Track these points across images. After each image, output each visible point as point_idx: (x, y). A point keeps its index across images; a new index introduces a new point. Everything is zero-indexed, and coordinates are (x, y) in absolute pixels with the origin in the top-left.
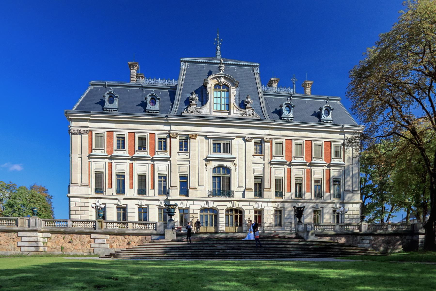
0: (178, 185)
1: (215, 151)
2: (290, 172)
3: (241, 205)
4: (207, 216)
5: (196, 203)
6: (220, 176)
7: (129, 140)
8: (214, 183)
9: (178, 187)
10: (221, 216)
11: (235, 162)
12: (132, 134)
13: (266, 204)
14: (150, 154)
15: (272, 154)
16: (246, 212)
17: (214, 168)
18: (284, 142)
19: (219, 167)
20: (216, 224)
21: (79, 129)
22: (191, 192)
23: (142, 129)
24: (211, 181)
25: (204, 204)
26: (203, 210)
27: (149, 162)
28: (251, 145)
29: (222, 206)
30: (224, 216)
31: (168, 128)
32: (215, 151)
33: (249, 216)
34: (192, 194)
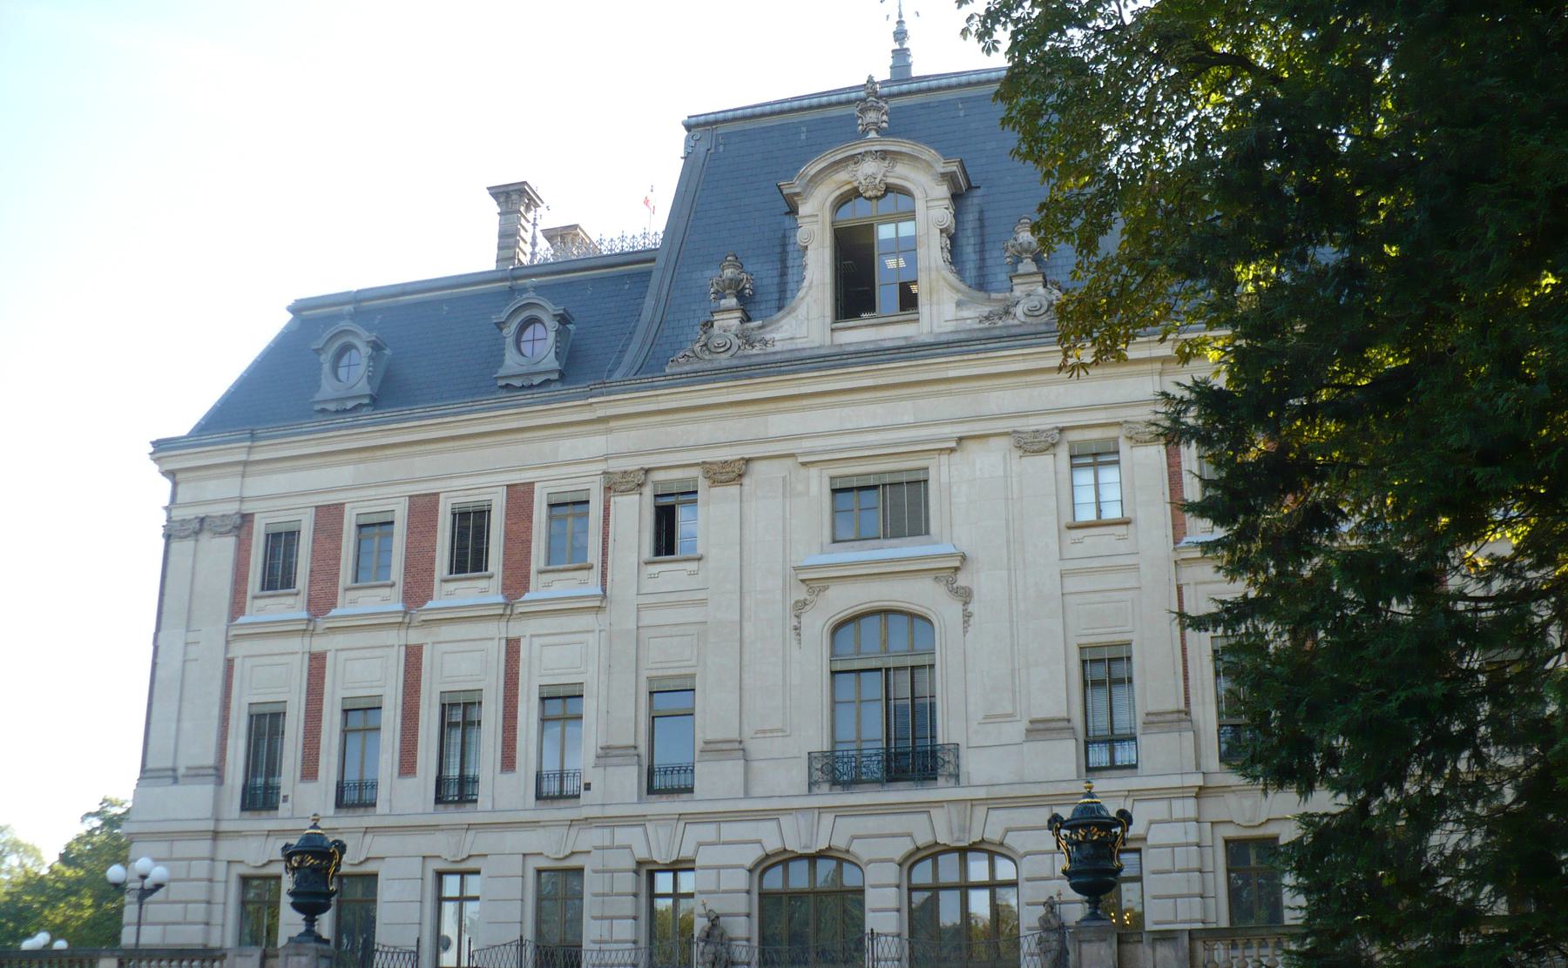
5: (730, 831)
10: (872, 898)
11: (962, 580)
21: (201, 511)
34: (715, 782)
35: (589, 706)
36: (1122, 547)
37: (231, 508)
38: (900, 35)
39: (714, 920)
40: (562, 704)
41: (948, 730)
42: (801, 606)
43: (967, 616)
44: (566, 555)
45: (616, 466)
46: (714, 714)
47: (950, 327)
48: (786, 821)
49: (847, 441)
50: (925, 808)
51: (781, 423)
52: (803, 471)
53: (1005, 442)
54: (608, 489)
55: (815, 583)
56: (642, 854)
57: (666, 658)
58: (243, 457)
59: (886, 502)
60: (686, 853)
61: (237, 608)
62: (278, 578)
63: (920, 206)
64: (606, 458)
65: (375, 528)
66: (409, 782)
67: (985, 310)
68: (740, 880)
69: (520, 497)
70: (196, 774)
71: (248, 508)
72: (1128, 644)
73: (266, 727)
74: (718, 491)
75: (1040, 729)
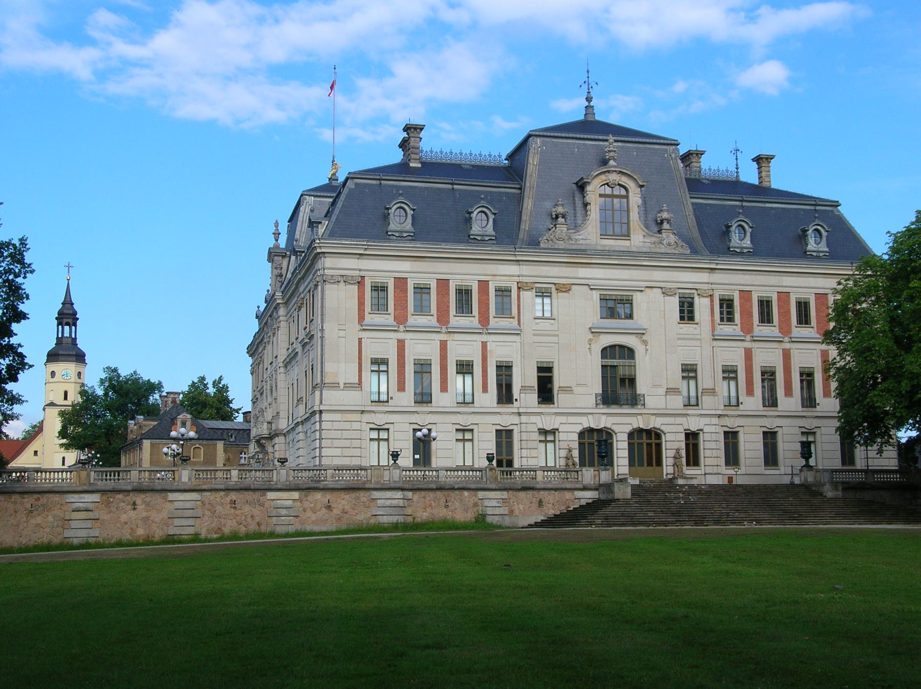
0: (534, 383)
5: (572, 419)
7: (438, 294)
8: (604, 378)
9: (536, 388)
11: (644, 338)
14: (480, 322)
17: (604, 350)
19: (613, 347)
22: (560, 398)
23: (465, 272)
26: (586, 434)
30: (625, 445)
31: (513, 269)
33: (672, 443)
35: (514, 369)
36: (696, 332)
37: (357, 273)
40: (505, 370)
41: (641, 388)
44: (504, 311)
45: (525, 280)
48: (590, 417)
49: (616, 283)
51: (583, 272)
52: (590, 292)
53: (659, 290)
54: (519, 288)
56: (541, 426)
57: (545, 356)
58: (362, 252)
59: (616, 306)
60: (556, 427)
61: (361, 318)
62: (380, 307)
63: (630, 194)
66: (445, 394)
68: (575, 437)
69: (484, 285)
70: (348, 386)
71: (362, 274)
74: (560, 294)
75: (671, 391)
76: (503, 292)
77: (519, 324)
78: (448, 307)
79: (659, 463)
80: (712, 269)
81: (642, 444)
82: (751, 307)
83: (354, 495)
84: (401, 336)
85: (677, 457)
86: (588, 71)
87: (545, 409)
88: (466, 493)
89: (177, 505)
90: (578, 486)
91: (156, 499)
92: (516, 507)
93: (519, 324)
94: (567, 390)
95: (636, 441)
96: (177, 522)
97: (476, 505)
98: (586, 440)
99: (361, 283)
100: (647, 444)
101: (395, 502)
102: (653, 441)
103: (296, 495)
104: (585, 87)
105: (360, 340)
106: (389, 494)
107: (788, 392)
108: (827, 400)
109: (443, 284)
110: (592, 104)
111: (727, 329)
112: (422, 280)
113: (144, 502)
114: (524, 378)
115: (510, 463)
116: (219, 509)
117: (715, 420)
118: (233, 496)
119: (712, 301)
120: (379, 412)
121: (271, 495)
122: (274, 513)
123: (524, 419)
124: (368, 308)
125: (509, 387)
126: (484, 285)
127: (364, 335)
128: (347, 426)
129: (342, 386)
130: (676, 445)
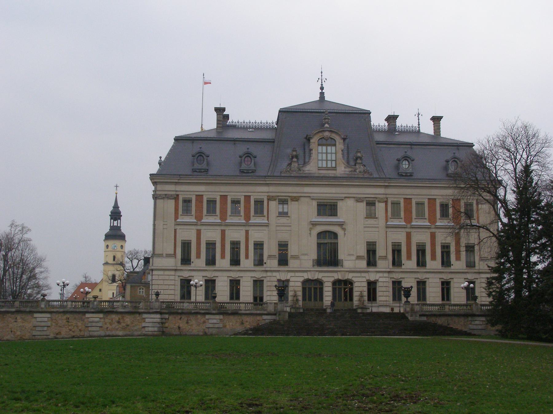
1: (319, 214)
2: (409, 236)
3: (350, 276)
4: (310, 289)
6: (326, 242)
10: (325, 289)
11: (344, 227)
12: (224, 198)
13: (379, 275)
15: (387, 216)
16: (356, 285)
18: (402, 201)
20: (321, 299)
24: (315, 247)
25: (306, 276)
26: (306, 282)
27: (244, 228)
28: (362, 206)
29: (328, 277)
30: (330, 289)
31: (265, 189)
32: (319, 214)
33: (360, 288)
34: (293, 264)
35: (265, 246)
36: (375, 223)
38: (322, 88)
39: (295, 292)
40: (259, 246)
41: (341, 256)
42: (311, 229)
43: (345, 234)
46: (292, 250)
47: (343, 172)
48: (309, 273)
50: (337, 272)
51: (307, 189)
53: (353, 199)
55: (314, 224)
56: (279, 278)
57: (283, 237)
58: (177, 181)
59: (328, 208)
61: (176, 217)
63: (337, 143)
64: (268, 192)
65: (212, 203)
67: (350, 169)
69: (247, 198)
70: (168, 256)
71: (178, 193)
72: (376, 242)
73: (186, 246)
74: (293, 202)
75: (359, 258)
76: (259, 203)
77: (268, 220)
78: (227, 211)
79: (351, 299)
80: (386, 186)
81: (341, 288)
82: (411, 207)
83: (133, 316)
84: (199, 227)
85: (361, 296)
86: (322, 72)
87: (282, 268)
88: (199, 316)
89: (38, 319)
90: (265, 312)
91: (28, 317)
92: (227, 324)
93: (268, 220)
94: (296, 257)
95: (337, 286)
96: (38, 329)
97: (204, 322)
98: (307, 286)
99: (176, 198)
100: (344, 288)
101: (155, 320)
102: (318, 286)
103: (101, 315)
104: (320, 81)
105: (175, 230)
106: (152, 316)
107: (433, 258)
108: (458, 262)
109: (224, 198)
110: (323, 91)
111: (396, 222)
112: (211, 196)
113: (21, 318)
114: (271, 249)
115: (261, 299)
116: (60, 322)
117: (386, 275)
118: (68, 316)
119: (386, 205)
120: (186, 270)
121: (88, 315)
122: (89, 325)
123: (269, 274)
124: (180, 212)
125: (262, 255)
126: (247, 198)
127: (178, 227)
128: (167, 277)
129: (164, 255)
130: (361, 289)
